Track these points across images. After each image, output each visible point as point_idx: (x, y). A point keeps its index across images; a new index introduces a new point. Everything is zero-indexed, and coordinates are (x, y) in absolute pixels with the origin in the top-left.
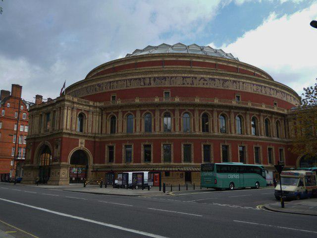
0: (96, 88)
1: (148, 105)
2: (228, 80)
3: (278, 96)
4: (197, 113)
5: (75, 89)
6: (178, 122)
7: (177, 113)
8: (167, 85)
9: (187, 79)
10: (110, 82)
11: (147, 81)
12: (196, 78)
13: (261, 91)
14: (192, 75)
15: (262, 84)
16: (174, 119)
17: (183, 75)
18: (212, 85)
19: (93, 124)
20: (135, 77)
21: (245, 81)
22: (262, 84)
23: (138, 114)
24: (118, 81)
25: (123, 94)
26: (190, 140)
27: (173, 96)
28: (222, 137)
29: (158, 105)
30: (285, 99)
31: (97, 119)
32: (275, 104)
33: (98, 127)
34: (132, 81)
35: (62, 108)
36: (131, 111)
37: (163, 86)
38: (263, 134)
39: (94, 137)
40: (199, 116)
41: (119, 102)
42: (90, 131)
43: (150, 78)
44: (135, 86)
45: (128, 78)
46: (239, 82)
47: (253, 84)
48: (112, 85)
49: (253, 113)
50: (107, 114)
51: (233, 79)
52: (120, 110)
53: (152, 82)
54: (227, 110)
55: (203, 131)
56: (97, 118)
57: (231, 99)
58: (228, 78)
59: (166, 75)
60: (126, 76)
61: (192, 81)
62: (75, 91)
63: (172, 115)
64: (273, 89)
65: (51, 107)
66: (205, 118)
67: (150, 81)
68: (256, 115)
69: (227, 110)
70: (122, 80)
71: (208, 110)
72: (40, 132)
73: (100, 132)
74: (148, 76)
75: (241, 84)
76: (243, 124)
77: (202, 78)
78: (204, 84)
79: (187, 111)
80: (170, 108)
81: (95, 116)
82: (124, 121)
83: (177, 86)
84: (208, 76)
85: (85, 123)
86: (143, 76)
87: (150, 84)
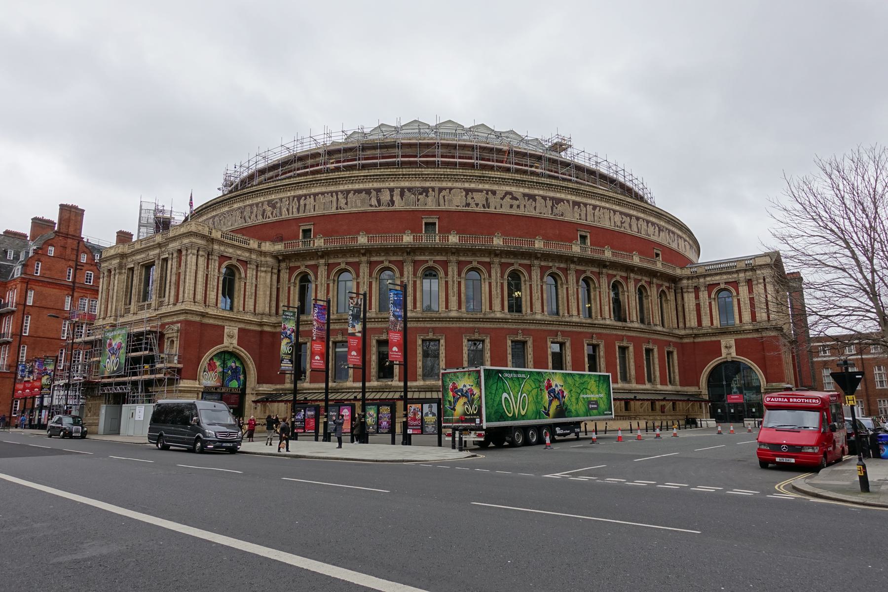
0: (264, 211)
1: (387, 251)
2: (562, 200)
3: (662, 238)
4: (496, 271)
5: (214, 213)
6: (456, 289)
7: (453, 269)
8: (431, 205)
9: (475, 195)
10: (299, 198)
11: (385, 197)
12: (494, 193)
13: (630, 226)
14: (487, 187)
15: (632, 212)
16: (447, 282)
17: (467, 185)
18: (528, 210)
19: (258, 294)
20: (357, 186)
21: (598, 203)
22: (632, 212)
23: (364, 269)
24: (317, 194)
25: (329, 224)
26: (481, 331)
27: (445, 231)
28: (551, 323)
29: (411, 251)
30: (674, 246)
31: (268, 280)
32: (657, 255)
33: (270, 300)
34: (351, 195)
35: (184, 253)
36: (347, 263)
38: (635, 319)
39: (261, 324)
40: (502, 276)
41: (319, 243)
42: (250, 306)
43: (391, 190)
44: (356, 205)
45: (341, 188)
46: (585, 205)
47: (615, 211)
48: (302, 202)
49: (615, 273)
50: (291, 270)
51: (574, 198)
52: (322, 261)
53: (397, 198)
54: (562, 265)
55: (511, 309)
56: (266, 279)
57: (571, 241)
58: (563, 196)
59: (427, 184)
61: (487, 199)
62: (214, 217)
63: (441, 274)
64: (653, 224)
65: (157, 251)
66: (515, 281)
67: (392, 196)
68: (621, 277)
69: (562, 265)
71: (520, 265)
72: (127, 311)
73: (274, 311)
74: (387, 185)
75: (590, 208)
76: (595, 296)
77: (507, 193)
78: (511, 206)
79: (475, 264)
80: (438, 258)
81: (263, 274)
82: (331, 285)
83: (453, 208)
84: (521, 190)
85: (239, 290)
86: (376, 185)
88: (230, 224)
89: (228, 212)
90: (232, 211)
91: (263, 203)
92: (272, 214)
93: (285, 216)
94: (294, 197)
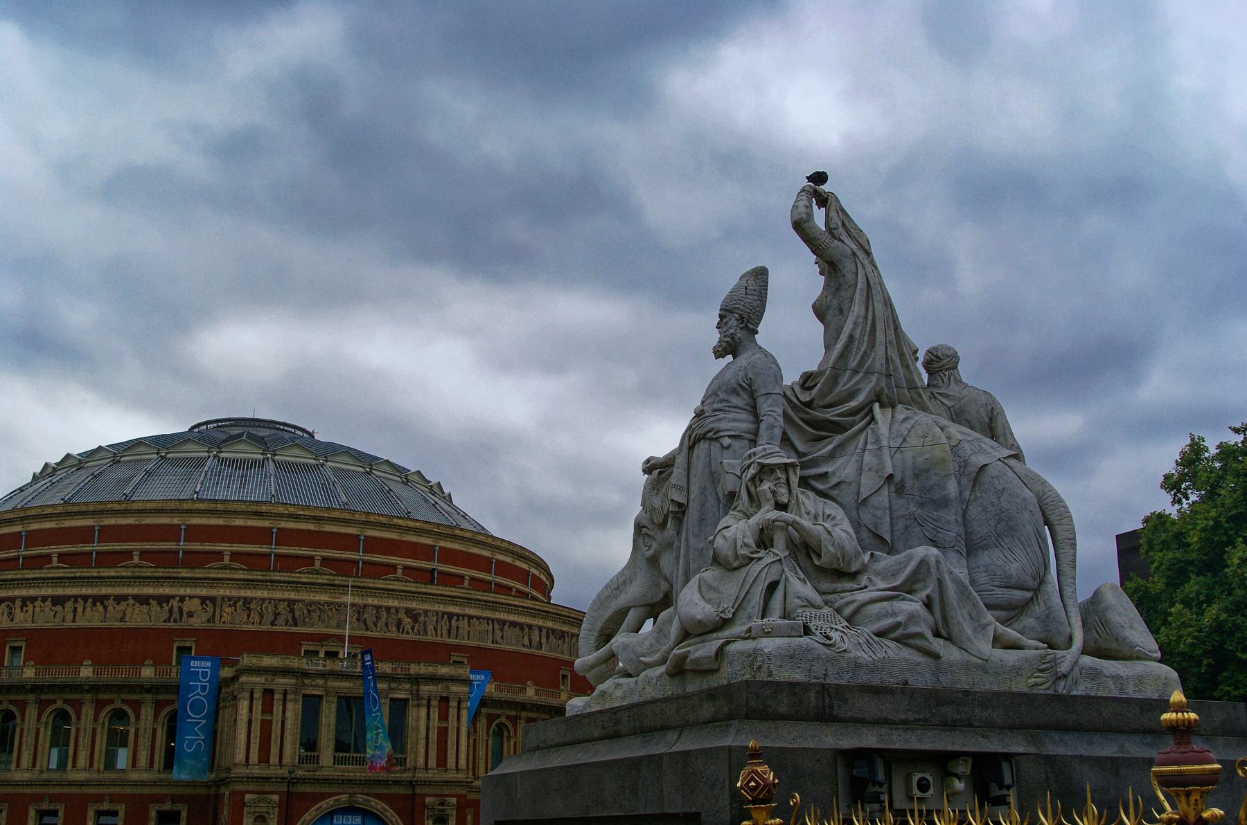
0: (399, 622)
10: (451, 616)
11: (536, 638)
20: (512, 618)
34: (506, 627)
35: (453, 703)
37: (560, 656)
43: (540, 629)
44: (511, 643)
48: (454, 623)
53: (544, 640)
59: (565, 628)
60: (494, 609)
70: (484, 619)
86: (528, 620)
87: (541, 644)
88: (334, 623)
89: (329, 604)
90: (340, 604)
91: (397, 609)
92: (413, 628)
93: (429, 638)
94: (444, 613)
